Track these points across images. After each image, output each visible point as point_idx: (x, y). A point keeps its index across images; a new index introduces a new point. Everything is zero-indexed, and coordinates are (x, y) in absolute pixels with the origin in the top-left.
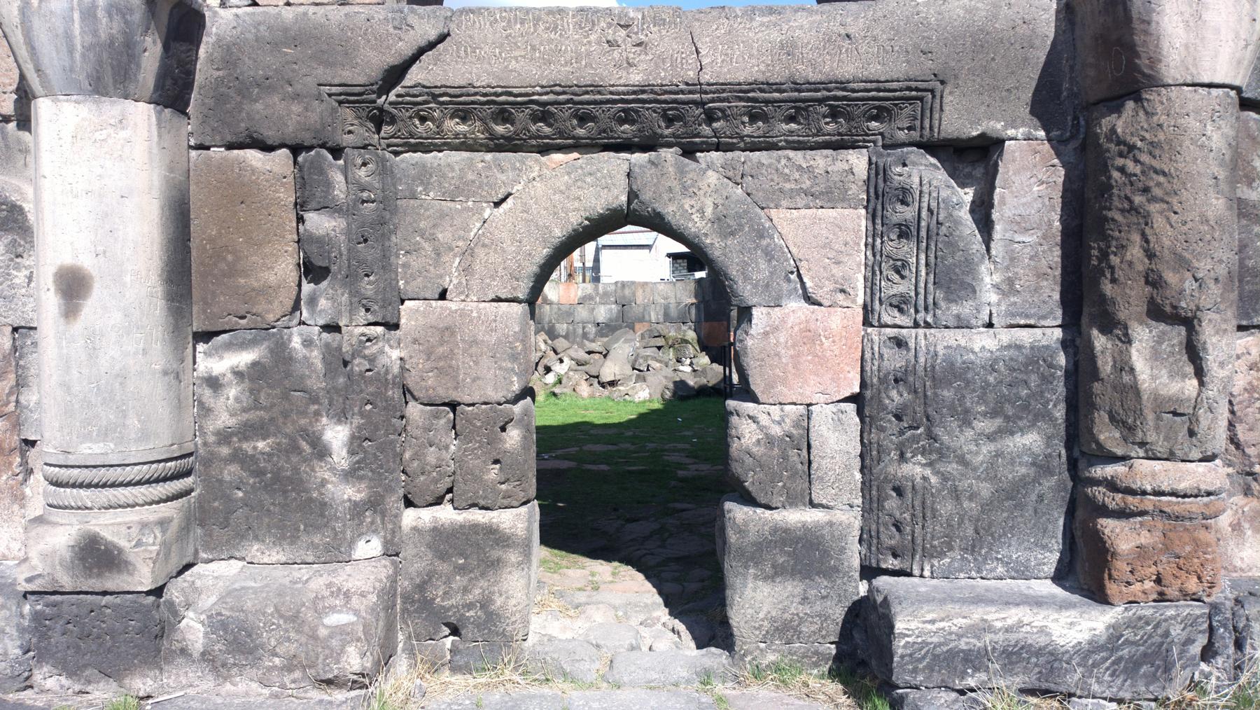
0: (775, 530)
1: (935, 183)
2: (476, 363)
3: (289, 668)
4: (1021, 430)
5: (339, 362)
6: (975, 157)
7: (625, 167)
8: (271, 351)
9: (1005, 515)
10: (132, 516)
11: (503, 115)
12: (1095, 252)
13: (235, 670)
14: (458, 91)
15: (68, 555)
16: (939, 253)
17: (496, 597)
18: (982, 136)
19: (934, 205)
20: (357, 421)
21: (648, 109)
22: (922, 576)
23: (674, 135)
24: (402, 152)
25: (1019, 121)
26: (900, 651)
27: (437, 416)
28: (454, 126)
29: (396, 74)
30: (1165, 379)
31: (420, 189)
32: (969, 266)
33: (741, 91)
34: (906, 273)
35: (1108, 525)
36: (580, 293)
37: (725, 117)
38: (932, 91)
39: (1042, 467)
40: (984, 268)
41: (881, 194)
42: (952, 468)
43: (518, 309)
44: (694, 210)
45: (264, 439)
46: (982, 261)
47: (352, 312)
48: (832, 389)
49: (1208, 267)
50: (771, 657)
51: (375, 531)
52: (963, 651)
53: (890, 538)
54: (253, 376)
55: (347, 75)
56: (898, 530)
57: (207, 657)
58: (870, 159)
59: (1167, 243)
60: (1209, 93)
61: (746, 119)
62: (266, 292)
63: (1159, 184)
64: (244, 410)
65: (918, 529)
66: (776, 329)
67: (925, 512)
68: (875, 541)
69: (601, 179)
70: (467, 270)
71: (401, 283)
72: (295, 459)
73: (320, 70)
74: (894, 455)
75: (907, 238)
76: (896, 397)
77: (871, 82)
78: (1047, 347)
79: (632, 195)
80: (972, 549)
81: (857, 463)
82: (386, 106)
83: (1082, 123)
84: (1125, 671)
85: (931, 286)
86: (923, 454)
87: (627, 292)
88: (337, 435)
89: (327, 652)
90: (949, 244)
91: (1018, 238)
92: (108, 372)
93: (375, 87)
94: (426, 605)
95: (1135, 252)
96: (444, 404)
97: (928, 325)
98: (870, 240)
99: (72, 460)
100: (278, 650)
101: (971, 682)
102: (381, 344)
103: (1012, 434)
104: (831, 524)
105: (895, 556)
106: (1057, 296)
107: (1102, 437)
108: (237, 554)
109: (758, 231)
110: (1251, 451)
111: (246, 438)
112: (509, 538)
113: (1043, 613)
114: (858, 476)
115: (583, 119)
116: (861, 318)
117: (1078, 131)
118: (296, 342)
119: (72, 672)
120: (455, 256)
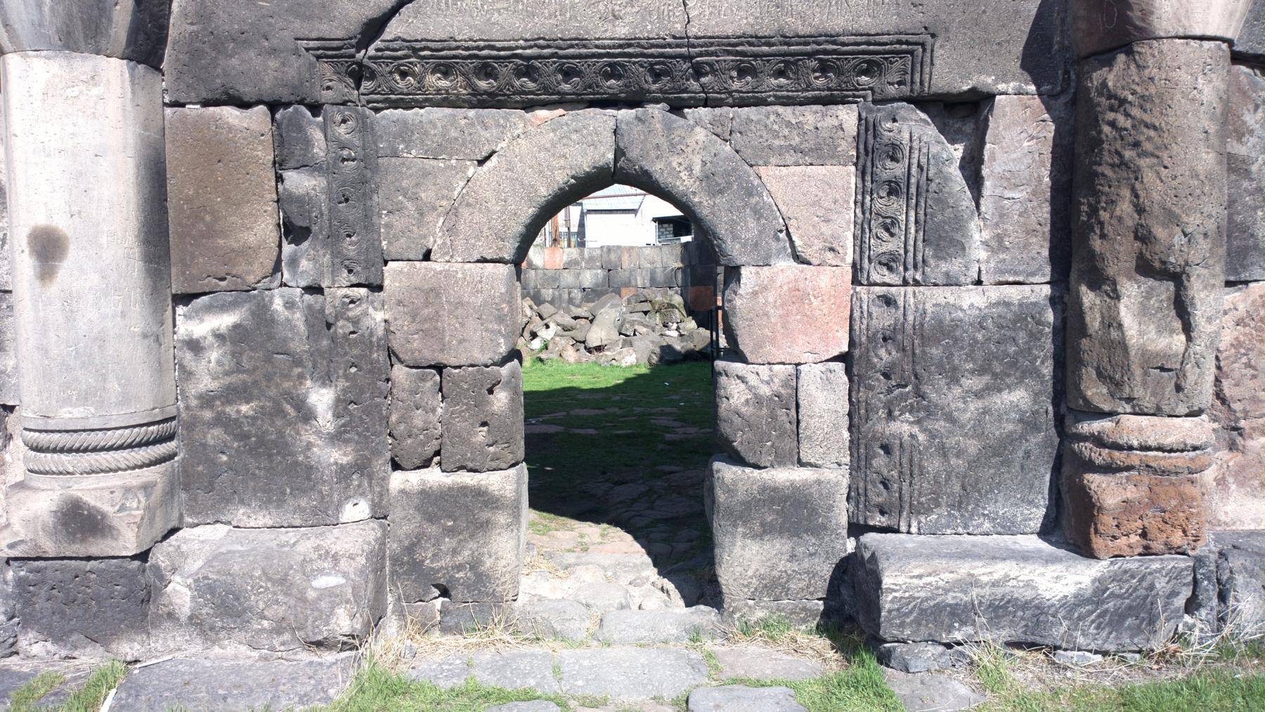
0: (764, 488)
1: (925, 139)
2: (462, 325)
3: (278, 631)
4: (1009, 387)
5: (322, 324)
6: (965, 113)
7: (612, 124)
8: (253, 313)
9: (992, 471)
10: (114, 480)
11: (486, 70)
12: (1085, 208)
13: (223, 634)
14: (439, 45)
15: (51, 521)
16: (929, 210)
17: (486, 558)
18: (973, 90)
19: (924, 161)
20: (342, 383)
21: (634, 63)
22: (909, 532)
23: (661, 91)
24: (382, 109)
25: (1010, 75)
26: (887, 606)
28: (435, 81)
29: (375, 27)
30: (1153, 335)
31: (401, 146)
32: (959, 223)
33: (728, 44)
34: (895, 230)
35: (1095, 481)
36: (565, 258)
37: (713, 72)
38: (923, 45)
39: (1029, 424)
40: (972, 225)
41: (871, 150)
42: (940, 425)
43: (504, 270)
44: (682, 168)
45: (248, 403)
46: (971, 218)
47: (334, 273)
48: (820, 348)
49: (1198, 222)
50: (760, 614)
51: (363, 494)
52: (950, 605)
53: (878, 495)
54: (235, 338)
55: (325, 29)
56: (885, 487)
57: (195, 621)
58: (860, 115)
59: (1156, 197)
60: (1201, 46)
61: (734, 74)
62: (247, 252)
63: (1149, 139)
64: (227, 374)
65: (905, 486)
66: (765, 288)
67: (913, 469)
68: (862, 499)
69: (588, 136)
70: (451, 230)
71: (384, 243)
72: (279, 423)
73: (297, 24)
74: (882, 413)
75: (897, 195)
76: (884, 356)
77: (861, 35)
78: (1035, 304)
79: (619, 153)
80: (959, 505)
81: (845, 422)
82: (366, 61)
83: (1073, 77)
84: (1110, 623)
85: (920, 244)
86: (911, 412)
87: (613, 256)
88: (321, 399)
89: (316, 614)
90: (939, 201)
93: (354, 41)
94: (415, 567)
95: (1125, 207)
96: (430, 367)
98: (859, 197)
99: (51, 425)
100: (266, 613)
101: (958, 636)
102: (364, 306)
103: (1000, 391)
104: (819, 482)
105: (882, 513)
106: (1046, 253)
107: (1089, 393)
108: (223, 518)
109: (747, 189)
110: (1236, 406)
111: (229, 402)
112: (498, 500)
113: (1029, 567)
114: (846, 435)
115: (568, 74)
116: (850, 277)
117: (1069, 85)
118: (278, 305)
119: (58, 637)
120: (439, 216)
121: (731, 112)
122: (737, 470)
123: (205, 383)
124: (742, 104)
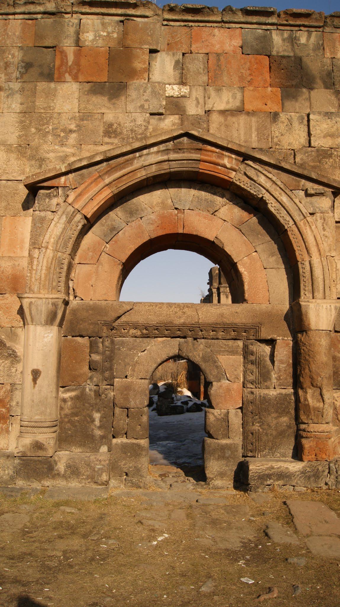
0: (219, 444)
3: (87, 478)
10: (46, 436)
12: (299, 370)
20: (102, 412)
27: (123, 411)
28: (132, 331)
30: (315, 403)
33: (209, 325)
39: (289, 427)
40: (272, 373)
53: (250, 447)
55: (105, 318)
56: (252, 444)
59: (314, 369)
67: (259, 439)
70: (133, 370)
73: (99, 317)
76: (251, 408)
80: (271, 449)
81: (241, 426)
88: (97, 416)
91: (281, 365)
95: (307, 371)
97: (259, 388)
111: (73, 417)
113: (287, 464)
114: (241, 430)
118: (87, 390)
123: (67, 411)
124: (213, 339)
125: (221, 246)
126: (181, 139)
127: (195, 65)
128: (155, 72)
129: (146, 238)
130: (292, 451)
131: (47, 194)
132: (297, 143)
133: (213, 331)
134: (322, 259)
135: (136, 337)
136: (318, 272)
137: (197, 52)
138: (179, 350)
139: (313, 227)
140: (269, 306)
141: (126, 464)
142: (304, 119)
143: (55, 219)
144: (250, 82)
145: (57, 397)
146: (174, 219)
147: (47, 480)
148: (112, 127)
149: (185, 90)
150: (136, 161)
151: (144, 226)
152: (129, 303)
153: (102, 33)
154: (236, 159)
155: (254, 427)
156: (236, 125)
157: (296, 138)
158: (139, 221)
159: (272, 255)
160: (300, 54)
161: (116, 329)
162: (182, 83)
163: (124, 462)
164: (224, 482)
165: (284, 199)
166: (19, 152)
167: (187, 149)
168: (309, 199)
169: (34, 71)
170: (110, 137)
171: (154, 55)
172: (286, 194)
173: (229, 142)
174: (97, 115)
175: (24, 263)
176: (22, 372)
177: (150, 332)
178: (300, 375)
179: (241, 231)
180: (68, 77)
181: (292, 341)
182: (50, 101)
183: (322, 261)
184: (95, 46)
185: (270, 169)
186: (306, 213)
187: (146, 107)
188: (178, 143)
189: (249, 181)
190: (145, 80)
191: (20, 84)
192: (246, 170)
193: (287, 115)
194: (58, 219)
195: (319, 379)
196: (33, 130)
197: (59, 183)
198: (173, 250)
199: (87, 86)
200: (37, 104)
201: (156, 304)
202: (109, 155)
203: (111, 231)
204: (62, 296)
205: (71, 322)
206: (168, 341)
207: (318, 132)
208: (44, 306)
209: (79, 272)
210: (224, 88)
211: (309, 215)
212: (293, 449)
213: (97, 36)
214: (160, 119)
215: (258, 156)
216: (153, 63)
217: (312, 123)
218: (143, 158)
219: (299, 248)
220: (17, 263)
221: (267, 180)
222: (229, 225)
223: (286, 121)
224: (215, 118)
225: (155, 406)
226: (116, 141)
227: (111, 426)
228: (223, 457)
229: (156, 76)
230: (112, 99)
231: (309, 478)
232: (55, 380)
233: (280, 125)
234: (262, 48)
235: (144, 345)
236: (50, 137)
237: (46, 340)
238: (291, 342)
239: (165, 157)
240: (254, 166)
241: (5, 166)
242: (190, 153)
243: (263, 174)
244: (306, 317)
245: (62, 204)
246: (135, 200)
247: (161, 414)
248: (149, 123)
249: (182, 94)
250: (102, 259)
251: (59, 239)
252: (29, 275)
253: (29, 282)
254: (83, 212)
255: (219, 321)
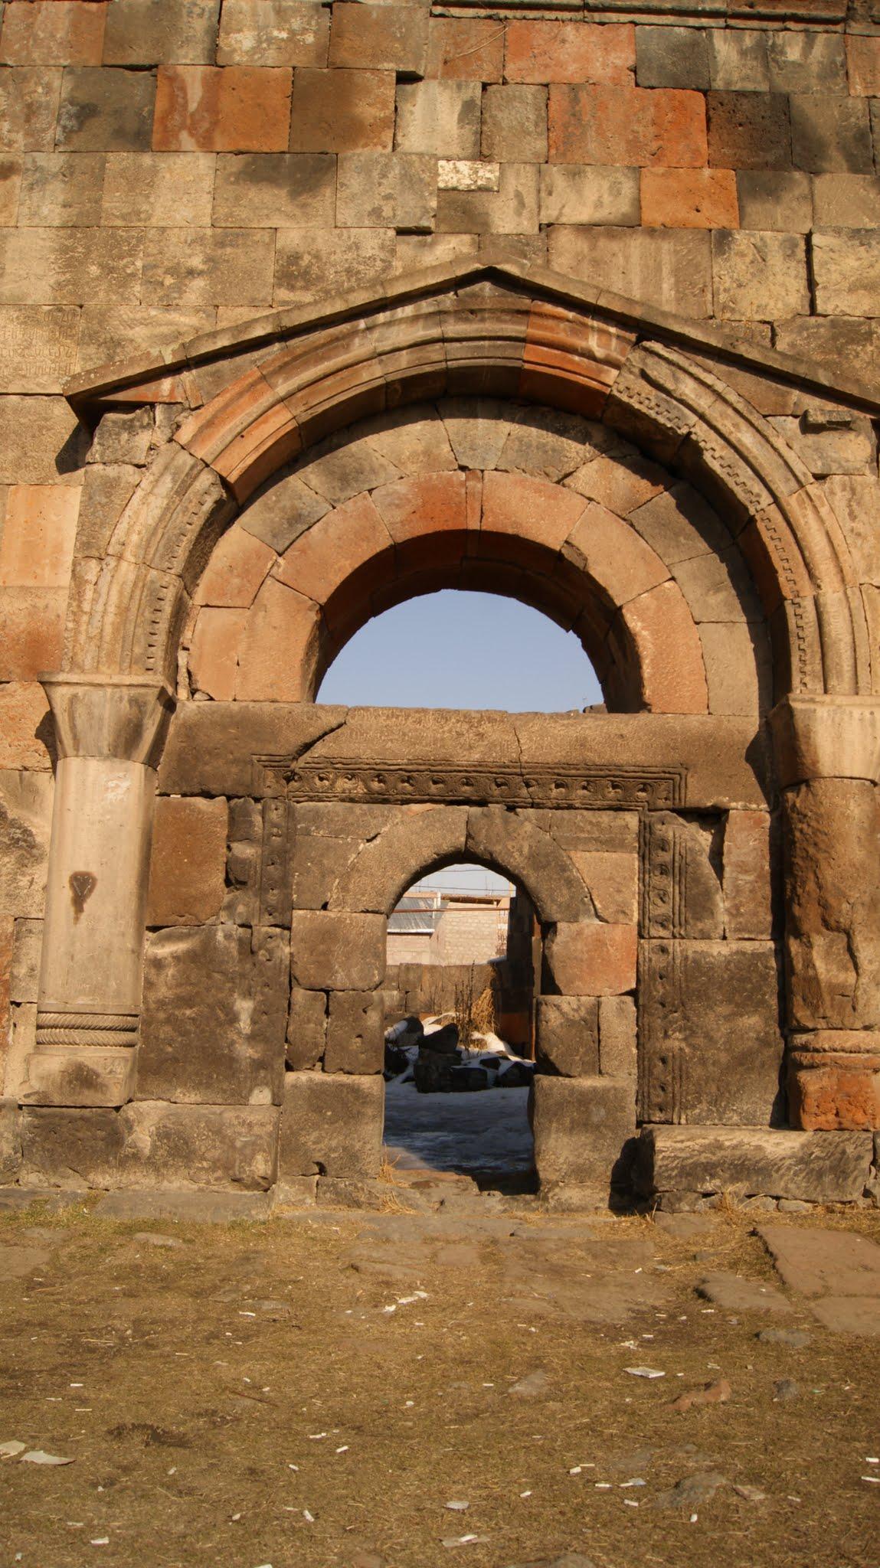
0: (572, 1091)
3: (213, 1169)
5: (248, 950)
12: (789, 887)
20: (259, 998)
27: (315, 999)
28: (343, 784)
30: (834, 972)
32: (708, 895)
33: (548, 768)
39: (764, 1042)
40: (718, 897)
41: (648, 844)
47: (261, 914)
51: (266, 1084)
53: (658, 1097)
55: (272, 749)
56: (663, 1088)
59: (830, 879)
67: (682, 1075)
69: (449, 825)
70: (344, 889)
76: (660, 990)
80: (714, 1102)
88: (244, 1007)
91: (741, 876)
92: (91, 953)
95: (811, 886)
103: (742, 1016)
107: (799, 1015)
111: (179, 1007)
114: (635, 1051)
118: (220, 936)
121: (550, 813)
122: (554, 1079)
123: (163, 992)
124: (558, 808)
125: (580, 564)
126: (476, 287)
127: (516, 112)
128: (411, 129)
129: (383, 543)
130: (770, 1107)
131: (125, 422)
132: (780, 305)
133: (558, 786)
134: (849, 592)
135: (352, 800)
136: (838, 626)
137: (519, 80)
138: (469, 836)
139: (824, 511)
140: (709, 719)
141: (321, 1142)
142: (796, 246)
143: (142, 485)
144: (656, 156)
145: (137, 952)
146: (458, 494)
147: (104, 1172)
148: (297, 264)
149: (488, 173)
150: (357, 341)
151: (378, 510)
152: (334, 709)
153: (276, 33)
154: (618, 337)
155: (669, 1043)
156: (621, 260)
157: (776, 294)
158: (365, 498)
159: (717, 588)
160: (785, 88)
161: (300, 778)
162: (481, 156)
163: (315, 1134)
164: (588, 1192)
165: (747, 438)
166: (56, 323)
167: (491, 311)
168: (811, 438)
169: (100, 126)
170: (292, 288)
171: (409, 88)
172: (752, 425)
173: (601, 292)
174: (262, 232)
175: (60, 603)
176: (46, 887)
177: (393, 785)
178: (792, 899)
179: (632, 525)
180: (186, 140)
181: (770, 813)
182: (140, 199)
183: (847, 598)
184: (259, 63)
185: (710, 363)
186: (805, 474)
187: (387, 212)
188: (467, 295)
189: (654, 392)
190: (385, 147)
191: (63, 157)
192: (645, 364)
193: (753, 236)
194: (151, 486)
195: (845, 906)
196: (94, 270)
197: (156, 395)
198: (456, 592)
199: (236, 163)
200: (106, 205)
201: (407, 713)
202: (289, 321)
203: (290, 525)
204: (158, 679)
205: (181, 758)
206: (439, 812)
207: (835, 277)
208: (108, 706)
209: (203, 627)
210: (588, 168)
211: (812, 480)
212: (775, 1104)
213: (264, 40)
214: (424, 245)
215: (677, 328)
216: (405, 108)
217: (817, 256)
218: (376, 334)
219: (786, 565)
220: (41, 604)
221: (701, 389)
222: (601, 509)
223: (751, 253)
224: (566, 243)
225: (410, 1071)
226: (307, 297)
227: (281, 1035)
228: (585, 1125)
229: (414, 138)
230: (300, 194)
231: (820, 1174)
232: (133, 905)
233: (736, 260)
234: (689, 73)
235: (373, 822)
236: (137, 288)
237: (110, 795)
238: (768, 816)
239: (435, 332)
240: (666, 355)
241: (17, 359)
242: (499, 320)
243: (691, 375)
244: (808, 743)
245: (164, 447)
246: (354, 447)
247: (424, 1086)
248: (393, 252)
249: (479, 183)
250: (267, 594)
251: (154, 533)
252: (71, 625)
253: (70, 645)
254: (218, 467)
255: (575, 757)
